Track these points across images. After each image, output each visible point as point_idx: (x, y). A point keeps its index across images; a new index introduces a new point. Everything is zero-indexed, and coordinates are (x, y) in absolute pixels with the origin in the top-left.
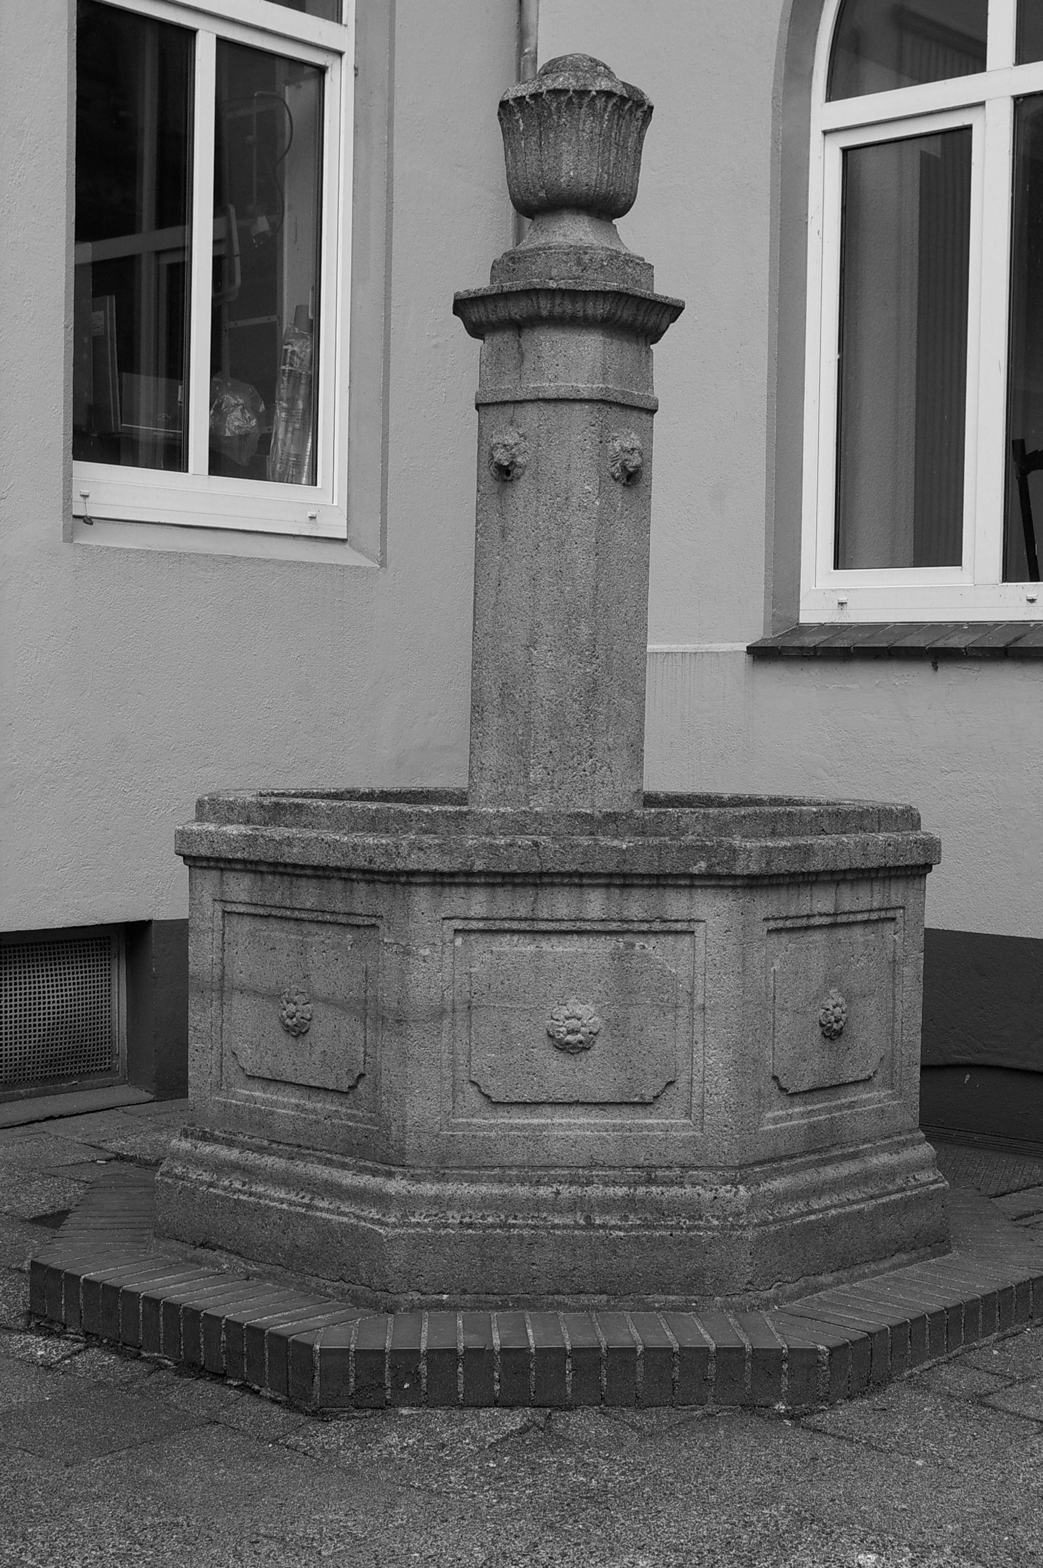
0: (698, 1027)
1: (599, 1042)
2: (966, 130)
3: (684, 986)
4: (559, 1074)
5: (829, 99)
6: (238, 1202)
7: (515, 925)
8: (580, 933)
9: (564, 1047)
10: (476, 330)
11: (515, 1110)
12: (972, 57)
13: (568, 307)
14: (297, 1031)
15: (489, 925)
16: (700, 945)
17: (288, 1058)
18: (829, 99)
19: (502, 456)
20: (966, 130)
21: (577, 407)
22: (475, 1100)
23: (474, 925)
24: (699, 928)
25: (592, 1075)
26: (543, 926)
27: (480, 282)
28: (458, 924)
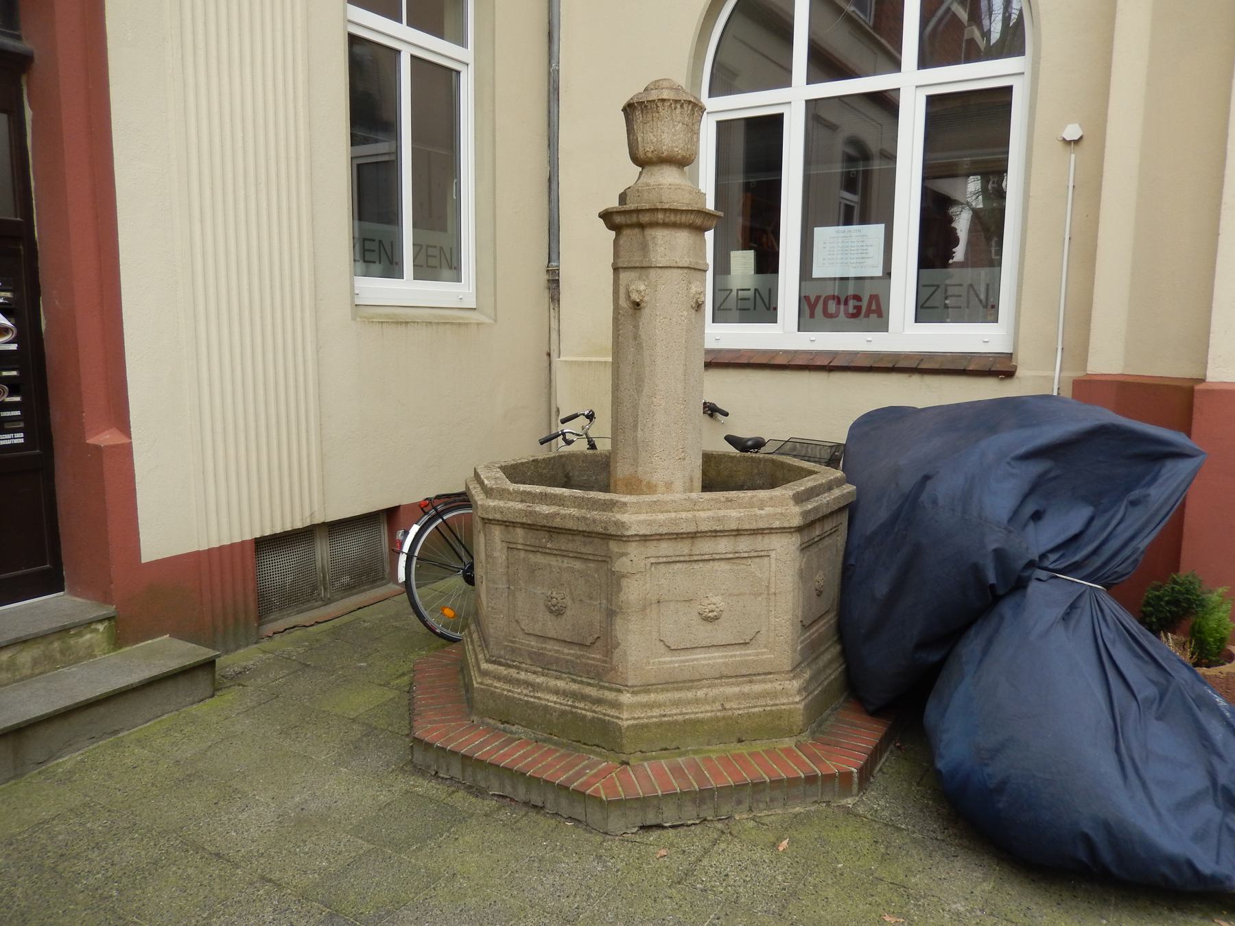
0: (772, 604)
1: (724, 615)
2: (781, 116)
3: (765, 583)
4: (704, 633)
5: (710, 96)
6: (527, 702)
7: (682, 559)
8: (713, 560)
9: (707, 619)
10: (611, 226)
11: (682, 653)
12: (784, 79)
13: (673, 218)
14: (557, 612)
15: (669, 559)
16: (773, 561)
17: (552, 627)
18: (710, 96)
19: (635, 297)
20: (781, 116)
21: (675, 271)
22: (663, 649)
23: (661, 560)
24: (773, 554)
25: (721, 633)
26: (695, 558)
27: (613, 203)
28: (653, 560)
